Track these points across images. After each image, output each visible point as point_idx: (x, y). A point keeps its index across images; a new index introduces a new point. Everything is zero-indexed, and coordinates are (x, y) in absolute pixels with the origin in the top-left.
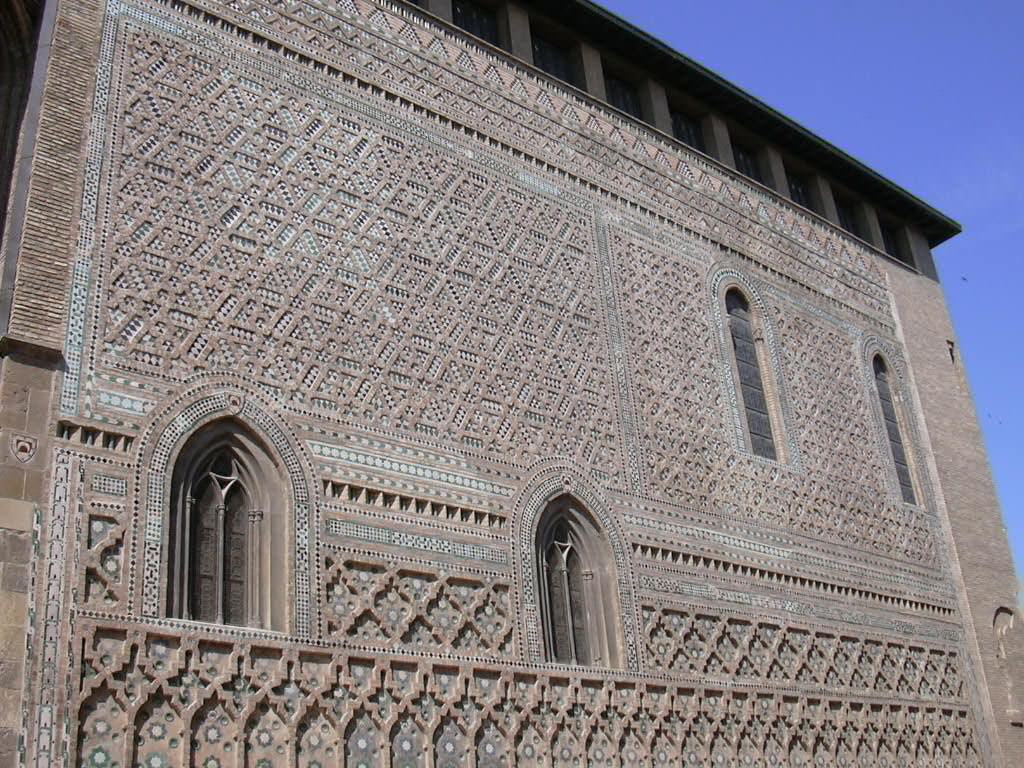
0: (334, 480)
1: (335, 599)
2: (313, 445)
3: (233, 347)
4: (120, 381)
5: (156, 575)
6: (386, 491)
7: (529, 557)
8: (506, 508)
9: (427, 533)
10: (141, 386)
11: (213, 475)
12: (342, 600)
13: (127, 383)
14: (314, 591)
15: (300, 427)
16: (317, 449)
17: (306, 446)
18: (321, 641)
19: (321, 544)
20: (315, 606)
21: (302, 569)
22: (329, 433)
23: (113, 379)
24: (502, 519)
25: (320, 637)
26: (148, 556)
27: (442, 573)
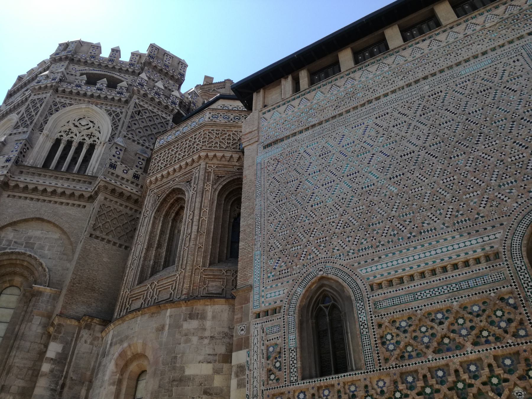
0: (376, 281)
1: (388, 342)
2: (361, 270)
3: (318, 247)
4: (274, 286)
5: (295, 362)
6: (440, 265)
7: (524, 268)
8: (496, 246)
9: (438, 285)
10: (282, 284)
11: (322, 305)
12: (392, 342)
13: (277, 285)
14: (373, 342)
15: (353, 265)
16: (364, 271)
17: (358, 272)
18: (381, 368)
19: (373, 316)
20: (374, 350)
21: (365, 333)
22: (369, 261)
23: (271, 287)
24: (497, 255)
25: (380, 366)
26: (291, 354)
27: (455, 303)
